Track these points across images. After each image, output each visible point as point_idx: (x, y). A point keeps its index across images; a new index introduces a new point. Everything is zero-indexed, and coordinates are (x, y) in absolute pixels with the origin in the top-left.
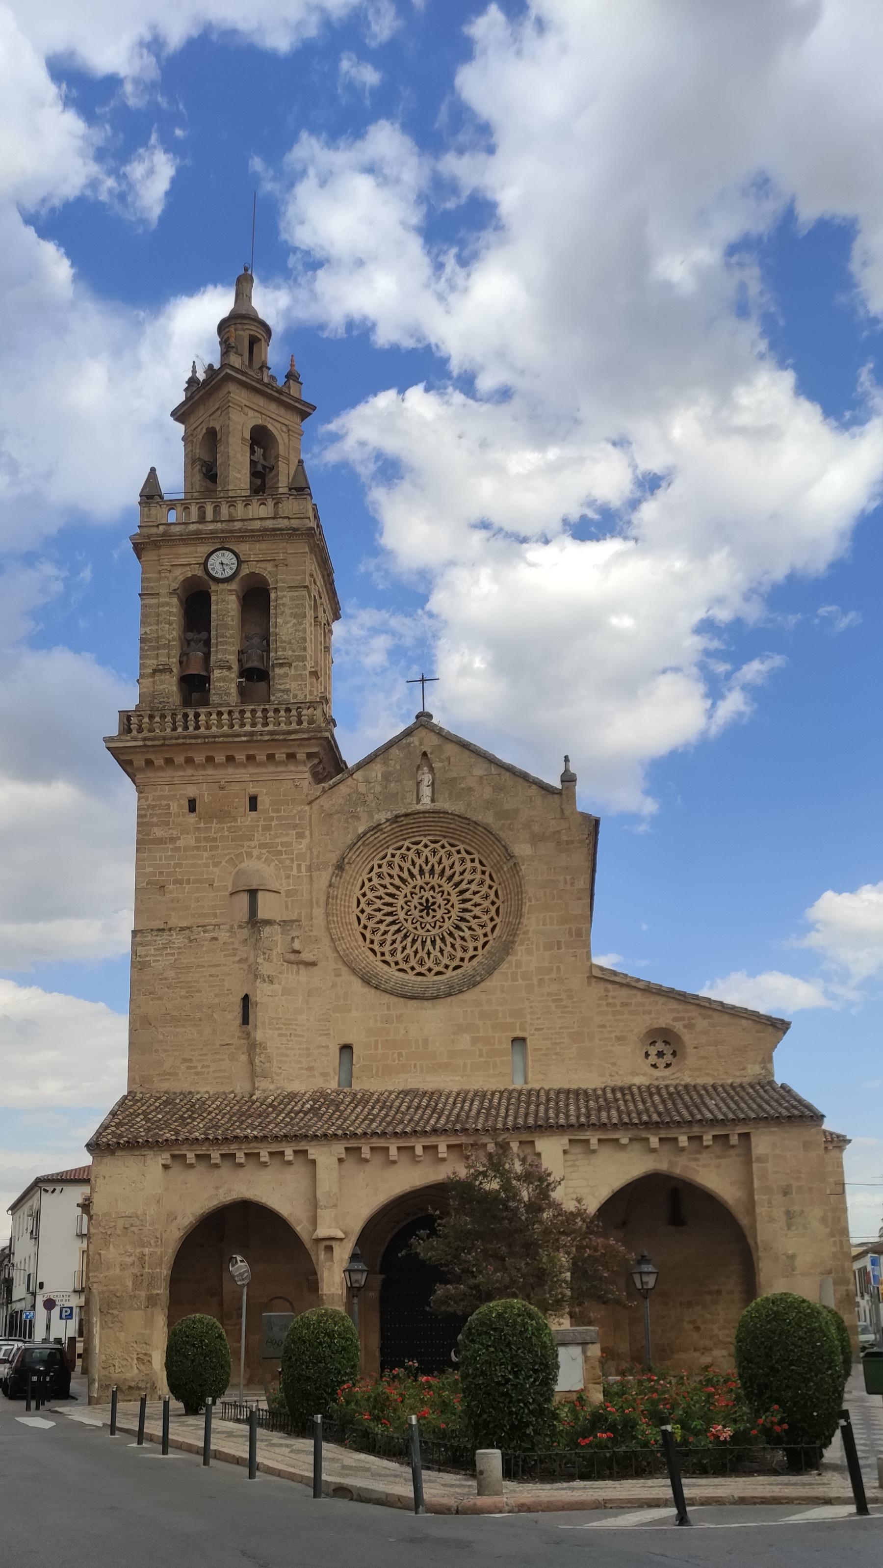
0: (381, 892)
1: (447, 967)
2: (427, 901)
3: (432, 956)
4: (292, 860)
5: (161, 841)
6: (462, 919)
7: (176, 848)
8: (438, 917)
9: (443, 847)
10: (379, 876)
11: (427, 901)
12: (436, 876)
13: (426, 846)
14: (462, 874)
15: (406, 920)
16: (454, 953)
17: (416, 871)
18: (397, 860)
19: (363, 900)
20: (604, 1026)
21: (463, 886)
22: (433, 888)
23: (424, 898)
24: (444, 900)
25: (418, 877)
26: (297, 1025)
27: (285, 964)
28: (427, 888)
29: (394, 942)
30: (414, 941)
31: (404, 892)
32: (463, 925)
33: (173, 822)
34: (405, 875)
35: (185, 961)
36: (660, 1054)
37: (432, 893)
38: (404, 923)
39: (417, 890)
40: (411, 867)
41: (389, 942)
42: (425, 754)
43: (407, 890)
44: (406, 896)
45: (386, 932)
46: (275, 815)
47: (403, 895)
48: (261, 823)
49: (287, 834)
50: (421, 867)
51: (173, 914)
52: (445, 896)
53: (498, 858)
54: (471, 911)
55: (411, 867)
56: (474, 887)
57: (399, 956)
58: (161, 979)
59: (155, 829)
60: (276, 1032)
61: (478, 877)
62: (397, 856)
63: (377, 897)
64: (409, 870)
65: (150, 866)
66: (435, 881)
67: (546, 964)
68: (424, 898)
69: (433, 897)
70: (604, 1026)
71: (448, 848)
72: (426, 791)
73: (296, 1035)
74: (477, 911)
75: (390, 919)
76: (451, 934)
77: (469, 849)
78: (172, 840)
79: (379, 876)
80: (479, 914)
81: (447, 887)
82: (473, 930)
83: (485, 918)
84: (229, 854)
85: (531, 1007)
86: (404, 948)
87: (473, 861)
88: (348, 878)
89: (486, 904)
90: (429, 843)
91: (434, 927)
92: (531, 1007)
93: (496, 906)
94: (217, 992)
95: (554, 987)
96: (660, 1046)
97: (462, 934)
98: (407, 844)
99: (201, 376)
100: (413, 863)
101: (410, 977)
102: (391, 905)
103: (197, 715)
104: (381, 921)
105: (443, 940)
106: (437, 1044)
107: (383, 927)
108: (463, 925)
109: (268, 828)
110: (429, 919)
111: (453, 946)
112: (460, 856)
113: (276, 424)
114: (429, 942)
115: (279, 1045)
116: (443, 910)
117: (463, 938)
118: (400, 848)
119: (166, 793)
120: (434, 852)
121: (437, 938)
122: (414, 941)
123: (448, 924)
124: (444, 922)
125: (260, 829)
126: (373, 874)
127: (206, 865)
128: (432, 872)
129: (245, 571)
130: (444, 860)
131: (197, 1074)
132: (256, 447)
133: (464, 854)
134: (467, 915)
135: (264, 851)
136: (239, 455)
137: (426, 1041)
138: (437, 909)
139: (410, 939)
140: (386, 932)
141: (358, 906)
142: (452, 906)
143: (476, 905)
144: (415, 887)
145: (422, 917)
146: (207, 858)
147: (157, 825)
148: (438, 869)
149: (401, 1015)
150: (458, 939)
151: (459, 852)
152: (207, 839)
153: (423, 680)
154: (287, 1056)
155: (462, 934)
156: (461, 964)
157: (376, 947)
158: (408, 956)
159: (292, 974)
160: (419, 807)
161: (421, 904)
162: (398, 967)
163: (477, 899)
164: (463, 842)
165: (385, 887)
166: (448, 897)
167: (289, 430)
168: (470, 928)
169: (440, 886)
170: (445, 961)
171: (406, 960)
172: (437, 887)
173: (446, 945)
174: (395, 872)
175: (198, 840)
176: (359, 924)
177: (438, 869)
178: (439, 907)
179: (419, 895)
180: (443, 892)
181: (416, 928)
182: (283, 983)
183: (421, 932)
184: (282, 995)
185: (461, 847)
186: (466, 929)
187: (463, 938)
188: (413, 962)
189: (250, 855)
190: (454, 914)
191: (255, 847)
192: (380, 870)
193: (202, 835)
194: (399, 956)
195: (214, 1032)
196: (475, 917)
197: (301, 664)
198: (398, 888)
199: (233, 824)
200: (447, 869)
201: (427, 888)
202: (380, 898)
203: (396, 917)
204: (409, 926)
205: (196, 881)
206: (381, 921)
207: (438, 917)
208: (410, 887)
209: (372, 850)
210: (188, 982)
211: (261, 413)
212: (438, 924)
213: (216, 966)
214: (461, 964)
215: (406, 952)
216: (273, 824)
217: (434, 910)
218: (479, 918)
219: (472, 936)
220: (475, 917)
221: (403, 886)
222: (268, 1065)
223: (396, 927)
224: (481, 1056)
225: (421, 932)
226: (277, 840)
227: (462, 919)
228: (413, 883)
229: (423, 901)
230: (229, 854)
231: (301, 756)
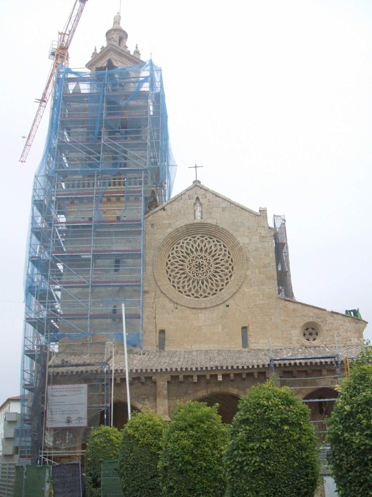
0: (178, 259)
2: (199, 263)
6: (216, 272)
8: (205, 271)
10: (177, 252)
11: (199, 263)
12: (203, 252)
13: (198, 239)
14: (215, 251)
15: (190, 272)
17: (194, 250)
18: (185, 245)
19: (169, 263)
21: (216, 257)
22: (202, 258)
23: (198, 262)
25: (195, 253)
29: (184, 282)
30: (193, 282)
31: (188, 259)
32: (216, 274)
34: (189, 252)
36: (311, 334)
37: (201, 260)
38: (189, 273)
39: (194, 259)
40: (192, 248)
41: (181, 282)
42: (198, 198)
43: (190, 258)
44: (189, 261)
45: (180, 278)
47: (188, 261)
50: (196, 248)
52: (208, 261)
55: (192, 248)
56: (221, 257)
57: (186, 289)
61: (223, 252)
62: (185, 243)
63: (176, 262)
64: (191, 249)
66: (203, 254)
68: (198, 262)
69: (202, 262)
72: (198, 214)
74: (223, 268)
75: (182, 272)
76: (211, 279)
79: (177, 252)
80: (224, 269)
81: (209, 257)
83: (227, 271)
86: (189, 285)
89: (227, 265)
90: (200, 238)
93: (232, 266)
96: (310, 330)
97: (216, 278)
99: (98, 51)
100: (193, 246)
102: (182, 265)
104: (178, 273)
105: (207, 281)
111: (212, 284)
114: (200, 282)
116: (207, 268)
117: (216, 281)
118: (186, 240)
120: (202, 241)
121: (204, 281)
122: (193, 282)
124: (207, 273)
128: (201, 250)
130: (207, 245)
133: (216, 242)
134: (218, 270)
139: (191, 281)
140: (180, 278)
142: (211, 266)
143: (222, 265)
145: (197, 271)
148: (204, 249)
150: (214, 281)
151: (214, 241)
153: (196, 167)
155: (216, 278)
156: (216, 292)
160: (196, 221)
161: (196, 265)
162: (186, 294)
163: (222, 263)
164: (216, 237)
169: (205, 257)
170: (208, 291)
171: (190, 290)
172: (204, 257)
174: (184, 250)
176: (167, 274)
177: (204, 249)
178: (205, 266)
179: (196, 261)
181: (194, 276)
183: (196, 277)
186: (218, 276)
188: (193, 291)
190: (212, 269)
192: (177, 249)
194: (186, 289)
196: (222, 271)
198: (185, 258)
200: (208, 249)
201: (199, 257)
202: (177, 262)
203: (185, 271)
204: (191, 274)
206: (178, 273)
207: (205, 271)
214: (216, 292)
215: (190, 287)
217: (203, 268)
220: (222, 271)
221: (188, 256)
223: (184, 276)
225: (196, 277)
228: (192, 256)
229: (198, 263)
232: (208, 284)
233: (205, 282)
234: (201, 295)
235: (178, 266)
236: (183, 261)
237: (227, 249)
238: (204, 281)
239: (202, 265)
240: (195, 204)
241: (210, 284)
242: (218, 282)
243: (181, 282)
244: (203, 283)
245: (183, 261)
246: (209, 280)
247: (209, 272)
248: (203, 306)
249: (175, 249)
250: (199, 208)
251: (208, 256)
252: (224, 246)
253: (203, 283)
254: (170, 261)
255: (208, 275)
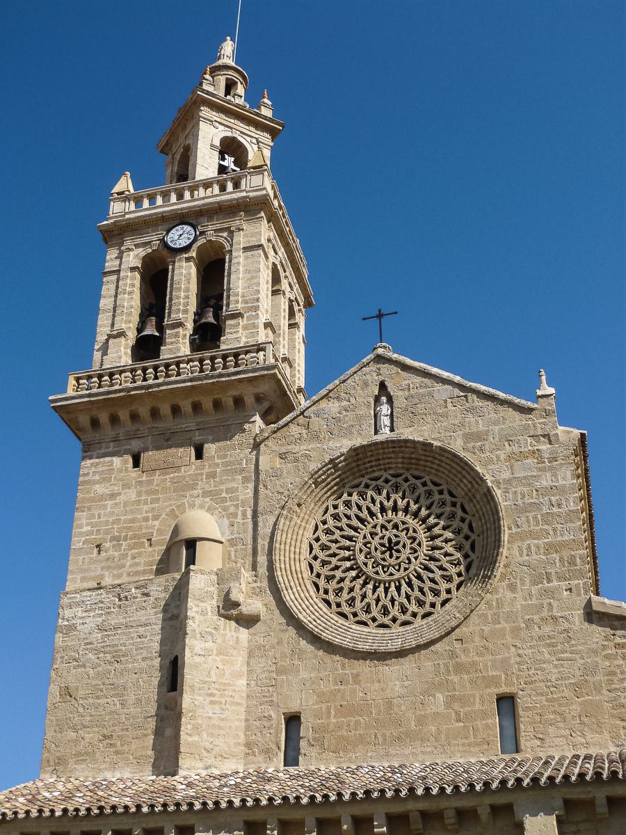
1: (414, 615)
2: (390, 540)
3: (396, 603)
4: (237, 506)
5: (102, 498)
6: (432, 559)
7: (116, 504)
8: (403, 556)
9: (406, 480)
11: (390, 540)
16: (422, 598)
17: (376, 509)
20: (614, 674)
22: (396, 526)
23: (386, 538)
24: (409, 538)
26: (235, 691)
27: (223, 619)
28: (389, 526)
31: (362, 533)
32: (432, 565)
33: (115, 478)
35: (112, 622)
40: (371, 505)
42: (383, 386)
43: (366, 530)
45: (342, 580)
46: (220, 461)
47: (361, 536)
48: (207, 470)
49: (233, 480)
50: (381, 503)
51: (107, 573)
52: (411, 533)
53: (469, 486)
54: (442, 548)
55: (371, 505)
58: (87, 644)
59: (97, 487)
60: (209, 699)
64: (368, 508)
65: (87, 524)
67: (534, 601)
68: (386, 538)
69: (396, 536)
70: (614, 674)
71: (413, 481)
73: (232, 704)
76: (419, 577)
77: (437, 480)
78: (113, 496)
82: (445, 570)
84: (171, 505)
85: (519, 655)
87: (441, 492)
88: (299, 522)
90: (390, 478)
91: (398, 570)
92: (519, 655)
94: (144, 655)
95: (547, 629)
97: (431, 575)
98: (365, 480)
101: (372, 629)
102: (348, 549)
103: (144, 370)
105: (410, 584)
106: (403, 708)
107: (338, 574)
108: (432, 565)
109: (212, 475)
110: (393, 561)
112: (426, 488)
113: (249, 139)
114: (393, 588)
115: (211, 715)
116: (408, 551)
117: (433, 581)
119: (111, 449)
121: (403, 582)
123: (415, 565)
125: (204, 477)
126: (328, 515)
127: (146, 519)
129: (201, 241)
131: (117, 753)
132: (226, 156)
133: (431, 486)
134: (437, 553)
135: (208, 499)
136: (207, 157)
137: (389, 704)
138: (402, 549)
140: (342, 580)
141: (311, 553)
144: (375, 527)
146: (147, 512)
147: (98, 482)
149: (358, 675)
152: (148, 493)
154: (220, 728)
155: (431, 575)
157: (331, 597)
158: (369, 605)
159: (230, 630)
160: (379, 438)
165: (341, 529)
166: (414, 535)
167: (258, 142)
168: (441, 568)
173: (413, 590)
175: (139, 494)
176: (312, 572)
178: (404, 546)
179: (381, 535)
180: (408, 529)
182: (219, 641)
183: (383, 576)
184: (217, 655)
185: (427, 479)
187: (433, 581)
189: (192, 506)
191: (198, 496)
193: (144, 489)
195: (139, 701)
196: (446, 554)
197: (254, 313)
198: (356, 529)
199: (176, 474)
201: (389, 526)
205: (135, 537)
206: (337, 568)
207: (403, 556)
208: (369, 526)
209: (326, 489)
210: (117, 645)
211: (231, 128)
212: (403, 565)
213: (146, 625)
216: (218, 470)
217: (398, 551)
218: (451, 555)
219: (443, 577)
220: (446, 554)
222: (196, 738)
224: (459, 720)
226: (223, 487)
227: (432, 559)
229: (386, 541)
230: (171, 505)
231: (249, 400)
232: (413, 590)
233: (404, 587)
234: (394, 620)
235: (337, 551)
236: (350, 538)
237: (459, 501)
238: (403, 582)
239: (397, 543)
240: (377, 400)
241: (416, 589)
242: (436, 583)
243: (346, 591)
244: (398, 589)
245: (350, 538)
246: (415, 581)
247: (413, 560)
248: (396, 645)
249: (331, 511)
250: (385, 409)
251: (411, 521)
252: (451, 494)
253: (398, 589)
254: (317, 540)
255: (412, 567)
